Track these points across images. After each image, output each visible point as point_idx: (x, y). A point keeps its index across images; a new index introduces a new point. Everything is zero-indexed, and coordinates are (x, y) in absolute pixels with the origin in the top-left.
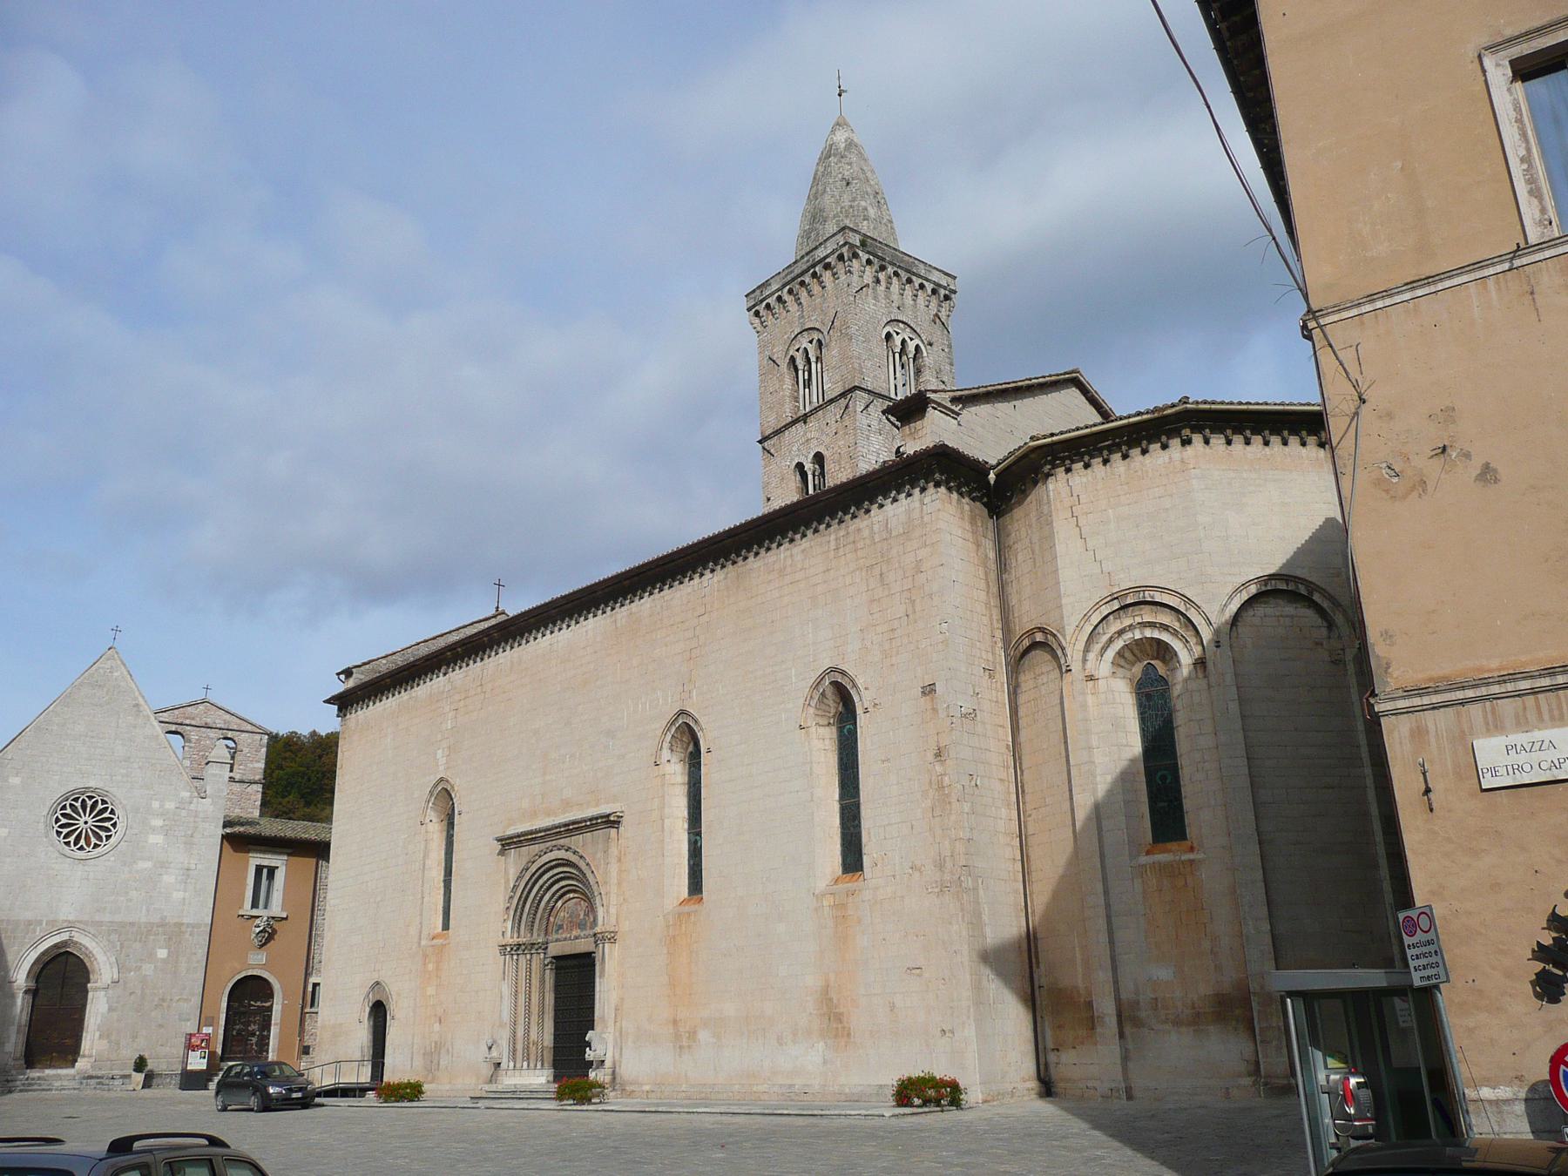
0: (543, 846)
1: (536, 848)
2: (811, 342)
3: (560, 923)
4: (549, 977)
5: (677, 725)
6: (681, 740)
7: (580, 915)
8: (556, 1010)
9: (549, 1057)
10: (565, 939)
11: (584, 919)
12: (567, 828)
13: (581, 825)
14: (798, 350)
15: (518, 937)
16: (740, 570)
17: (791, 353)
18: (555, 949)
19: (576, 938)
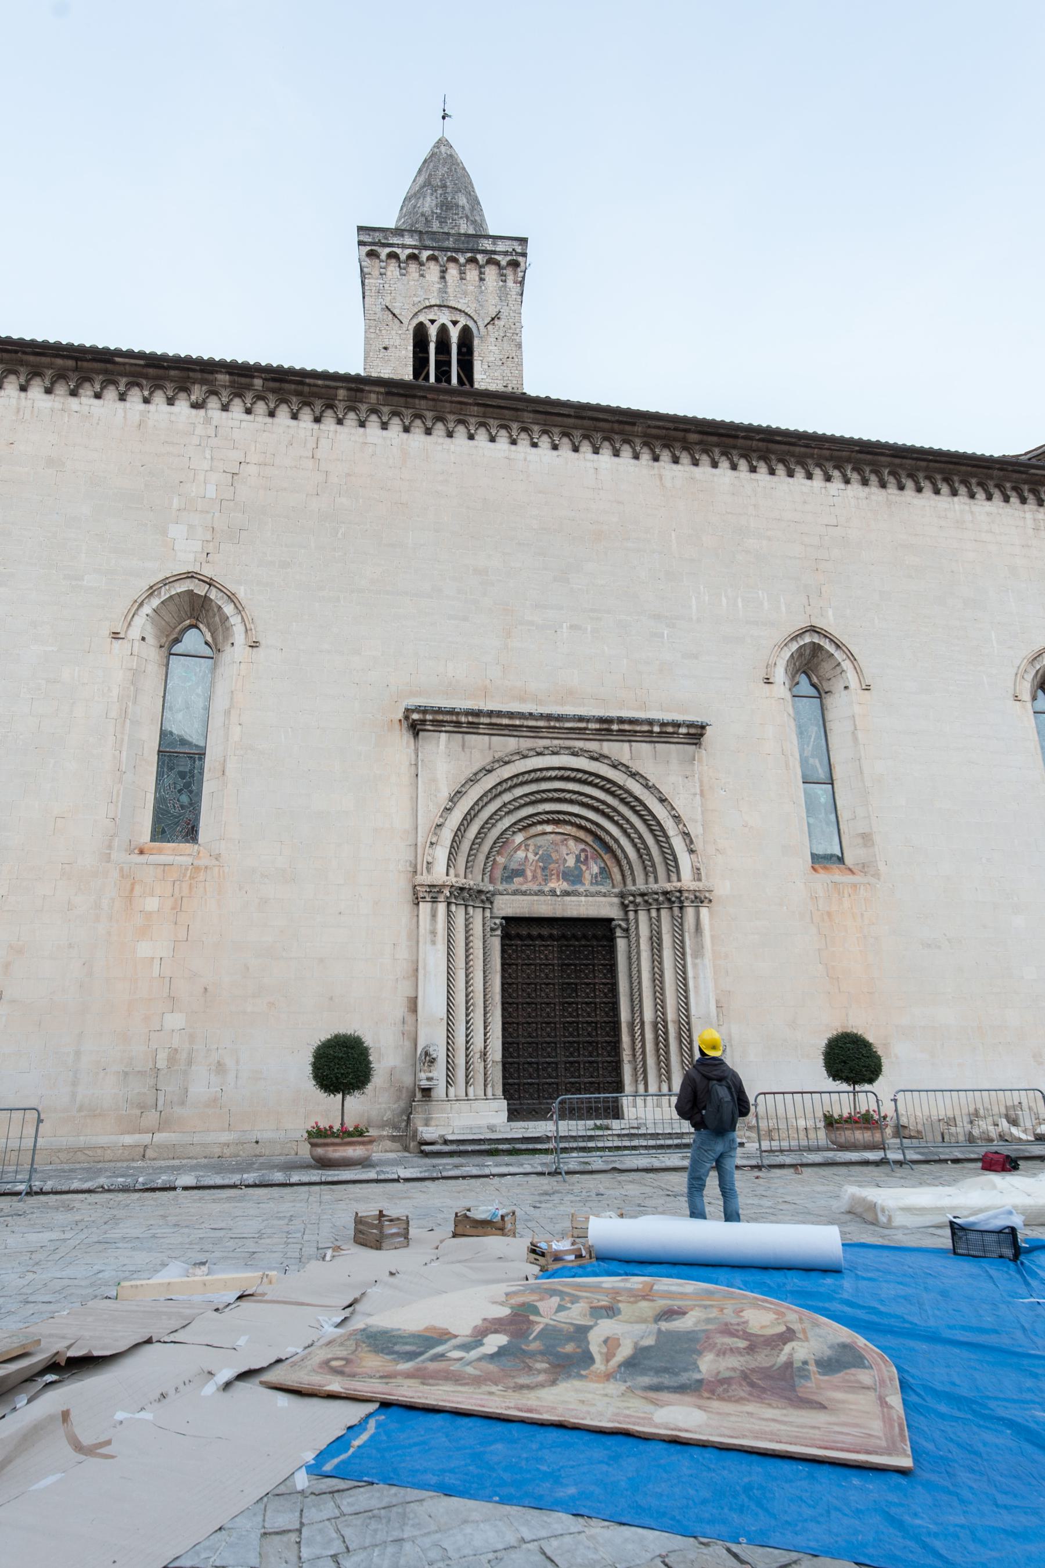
0: (525, 744)
1: (512, 744)
2: (455, 323)
3: (513, 866)
4: (496, 943)
5: (802, 643)
6: (795, 664)
7: (565, 860)
8: (504, 1004)
9: (497, 1074)
10: (540, 893)
11: (577, 867)
12: (605, 726)
13: (638, 728)
14: (433, 322)
15: (456, 876)
16: (893, 498)
17: (422, 318)
18: (509, 906)
19: (566, 893)
